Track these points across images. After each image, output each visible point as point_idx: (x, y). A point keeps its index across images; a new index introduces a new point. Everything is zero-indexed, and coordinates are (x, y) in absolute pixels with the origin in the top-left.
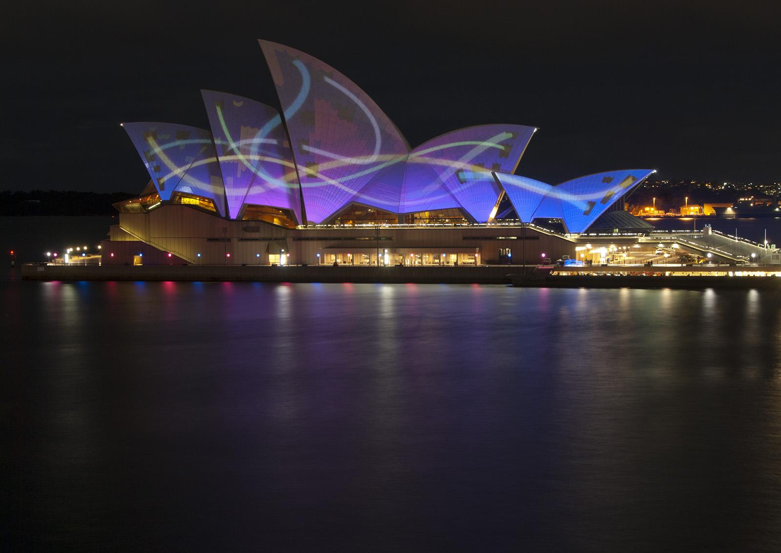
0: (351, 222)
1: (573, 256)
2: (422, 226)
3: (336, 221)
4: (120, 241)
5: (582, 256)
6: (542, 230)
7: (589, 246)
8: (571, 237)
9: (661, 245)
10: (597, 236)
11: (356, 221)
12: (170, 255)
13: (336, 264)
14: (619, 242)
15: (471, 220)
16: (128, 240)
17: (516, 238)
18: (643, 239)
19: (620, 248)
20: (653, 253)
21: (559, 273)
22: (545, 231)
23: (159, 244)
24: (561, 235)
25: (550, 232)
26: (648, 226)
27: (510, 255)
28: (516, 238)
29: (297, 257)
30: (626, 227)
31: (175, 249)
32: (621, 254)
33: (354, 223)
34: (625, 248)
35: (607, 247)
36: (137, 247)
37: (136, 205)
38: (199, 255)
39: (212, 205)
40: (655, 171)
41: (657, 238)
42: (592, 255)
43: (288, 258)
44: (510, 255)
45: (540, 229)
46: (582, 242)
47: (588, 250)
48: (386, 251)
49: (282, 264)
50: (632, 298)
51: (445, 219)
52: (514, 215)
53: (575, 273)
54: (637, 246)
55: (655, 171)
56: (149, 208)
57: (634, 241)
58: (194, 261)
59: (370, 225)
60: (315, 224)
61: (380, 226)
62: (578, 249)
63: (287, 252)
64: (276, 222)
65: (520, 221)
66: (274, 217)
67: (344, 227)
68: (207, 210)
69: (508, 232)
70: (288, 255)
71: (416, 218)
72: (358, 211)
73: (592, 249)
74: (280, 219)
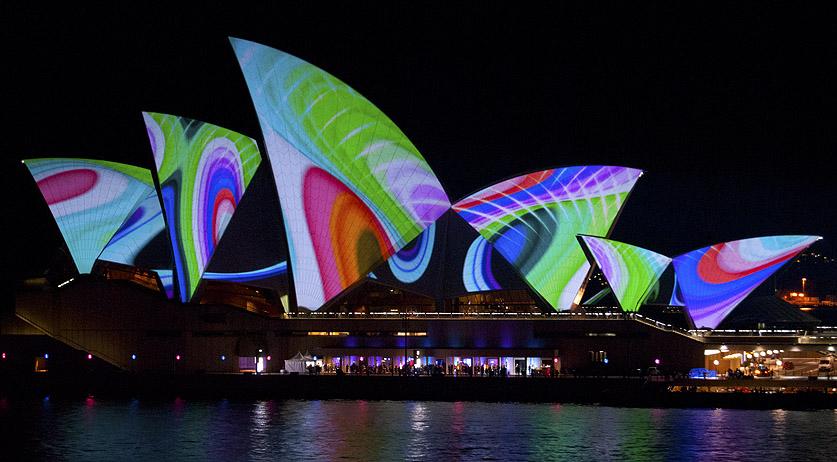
0: (363, 308)
1: (700, 362)
2: (471, 315)
3: (341, 307)
4: (15, 336)
5: (716, 362)
6: (654, 324)
7: (724, 348)
8: (695, 335)
9: (831, 349)
10: (737, 333)
11: (371, 308)
12: (90, 357)
13: (339, 371)
14: (768, 342)
15: (546, 307)
16: (27, 332)
17: (613, 335)
18: (804, 339)
19: (770, 352)
20: (816, 361)
21: (684, 389)
22: (659, 325)
23: (74, 340)
24: (682, 331)
25: (666, 327)
26: (811, 319)
27: (606, 361)
28: (613, 335)
29: (275, 365)
30: (779, 321)
31: (96, 349)
32: (768, 361)
33: (368, 312)
34: (776, 352)
35: (749, 351)
36: (43, 343)
37: (41, 281)
38: (134, 357)
39: (154, 281)
40: (821, 238)
41: (825, 339)
42: (729, 361)
43: (267, 363)
44: (606, 361)
45: (651, 323)
46: (714, 342)
47: (723, 354)
48: (418, 353)
49: (259, 371)
50: (789, 423)
51: (505, 305)
52: (611, 301)
53: (706, 389)
54: (796, 349)
55: (821, 238)
56: (28, 281)
57: (793, 342)
58: (125, 366)
59: (394, 312)
60: (308, 312)
61: (407, 315)
62: (708, 352)
63: (264, 355)
64: (250, 307)
65: (620, 309)
66: (247, 300)
67: (353, 315)
68: (147, 289)
69: (605, 325)
70: (269, 358)
71: (462, 303)
72: (374, 291)
73: (727, 354)
74: (256, 303)
